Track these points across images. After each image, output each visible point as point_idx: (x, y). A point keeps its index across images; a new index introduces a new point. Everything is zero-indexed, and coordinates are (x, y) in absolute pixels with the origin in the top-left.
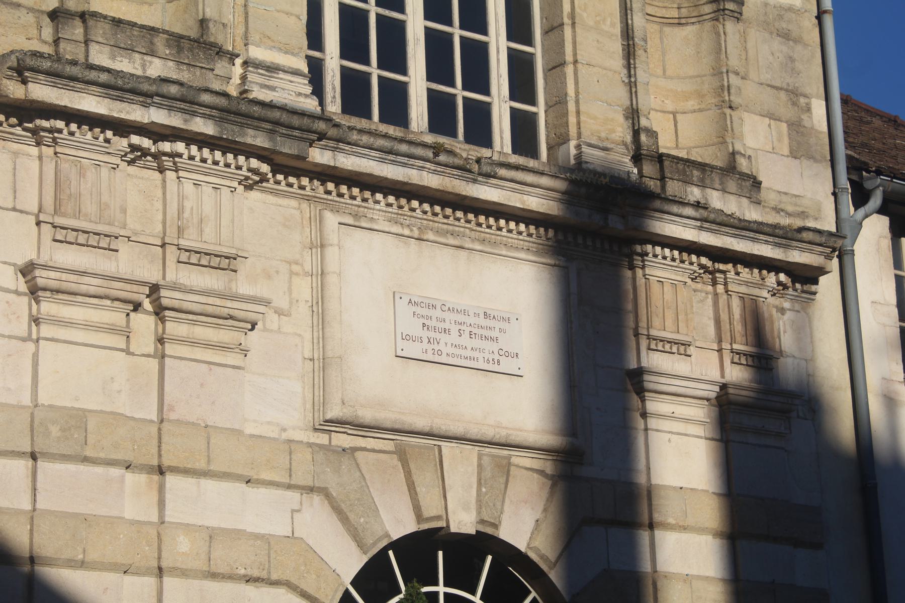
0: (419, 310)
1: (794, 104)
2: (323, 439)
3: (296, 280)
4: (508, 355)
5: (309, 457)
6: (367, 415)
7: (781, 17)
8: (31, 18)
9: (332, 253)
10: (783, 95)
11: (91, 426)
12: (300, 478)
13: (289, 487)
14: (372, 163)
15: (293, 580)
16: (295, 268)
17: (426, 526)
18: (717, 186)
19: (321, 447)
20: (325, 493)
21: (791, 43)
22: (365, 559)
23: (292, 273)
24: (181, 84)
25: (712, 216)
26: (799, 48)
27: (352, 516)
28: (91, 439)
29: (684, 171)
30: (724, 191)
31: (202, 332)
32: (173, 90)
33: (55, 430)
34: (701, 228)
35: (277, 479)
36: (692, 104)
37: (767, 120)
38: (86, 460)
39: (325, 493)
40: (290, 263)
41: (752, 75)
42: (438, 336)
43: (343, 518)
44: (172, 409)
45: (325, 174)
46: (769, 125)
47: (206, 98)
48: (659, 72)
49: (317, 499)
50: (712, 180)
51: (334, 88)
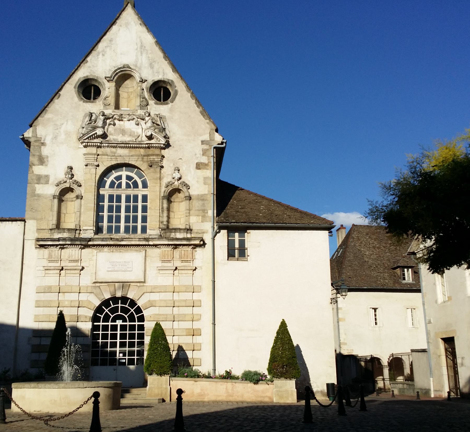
0: (111, 263)
1: (204, 212)
2: (94, 285)
4: (129, 268)
5: (91, 288)
6: (100, 281)
7: (202, 197)
8: (47, 231)
10: (201, 211)
13: (87, 293)
14: (100, 242)
15: (86, 306)
16: (90, 260)
18: (178, 232)
19: (93, 286)
21: (204, 201)
22: (101, 302)
24: (62, 238)
25: (170, 239)
27: (98, 296)
28: (52, 290)
29: (171, 231)
30: (180, 232)
31: (72, 272)
32: (61, 239)
34: (169, 241)
36: (183, 216)
37: (196, 217)
38: (51, 292)
40: (89, 259)
42: (115, 267)
43: (97, 297)
45: (94, 245)
46: (197, 218)
47: (67, 239)
48: (178, 211)
50: (177, 231)
51: (105, 229)
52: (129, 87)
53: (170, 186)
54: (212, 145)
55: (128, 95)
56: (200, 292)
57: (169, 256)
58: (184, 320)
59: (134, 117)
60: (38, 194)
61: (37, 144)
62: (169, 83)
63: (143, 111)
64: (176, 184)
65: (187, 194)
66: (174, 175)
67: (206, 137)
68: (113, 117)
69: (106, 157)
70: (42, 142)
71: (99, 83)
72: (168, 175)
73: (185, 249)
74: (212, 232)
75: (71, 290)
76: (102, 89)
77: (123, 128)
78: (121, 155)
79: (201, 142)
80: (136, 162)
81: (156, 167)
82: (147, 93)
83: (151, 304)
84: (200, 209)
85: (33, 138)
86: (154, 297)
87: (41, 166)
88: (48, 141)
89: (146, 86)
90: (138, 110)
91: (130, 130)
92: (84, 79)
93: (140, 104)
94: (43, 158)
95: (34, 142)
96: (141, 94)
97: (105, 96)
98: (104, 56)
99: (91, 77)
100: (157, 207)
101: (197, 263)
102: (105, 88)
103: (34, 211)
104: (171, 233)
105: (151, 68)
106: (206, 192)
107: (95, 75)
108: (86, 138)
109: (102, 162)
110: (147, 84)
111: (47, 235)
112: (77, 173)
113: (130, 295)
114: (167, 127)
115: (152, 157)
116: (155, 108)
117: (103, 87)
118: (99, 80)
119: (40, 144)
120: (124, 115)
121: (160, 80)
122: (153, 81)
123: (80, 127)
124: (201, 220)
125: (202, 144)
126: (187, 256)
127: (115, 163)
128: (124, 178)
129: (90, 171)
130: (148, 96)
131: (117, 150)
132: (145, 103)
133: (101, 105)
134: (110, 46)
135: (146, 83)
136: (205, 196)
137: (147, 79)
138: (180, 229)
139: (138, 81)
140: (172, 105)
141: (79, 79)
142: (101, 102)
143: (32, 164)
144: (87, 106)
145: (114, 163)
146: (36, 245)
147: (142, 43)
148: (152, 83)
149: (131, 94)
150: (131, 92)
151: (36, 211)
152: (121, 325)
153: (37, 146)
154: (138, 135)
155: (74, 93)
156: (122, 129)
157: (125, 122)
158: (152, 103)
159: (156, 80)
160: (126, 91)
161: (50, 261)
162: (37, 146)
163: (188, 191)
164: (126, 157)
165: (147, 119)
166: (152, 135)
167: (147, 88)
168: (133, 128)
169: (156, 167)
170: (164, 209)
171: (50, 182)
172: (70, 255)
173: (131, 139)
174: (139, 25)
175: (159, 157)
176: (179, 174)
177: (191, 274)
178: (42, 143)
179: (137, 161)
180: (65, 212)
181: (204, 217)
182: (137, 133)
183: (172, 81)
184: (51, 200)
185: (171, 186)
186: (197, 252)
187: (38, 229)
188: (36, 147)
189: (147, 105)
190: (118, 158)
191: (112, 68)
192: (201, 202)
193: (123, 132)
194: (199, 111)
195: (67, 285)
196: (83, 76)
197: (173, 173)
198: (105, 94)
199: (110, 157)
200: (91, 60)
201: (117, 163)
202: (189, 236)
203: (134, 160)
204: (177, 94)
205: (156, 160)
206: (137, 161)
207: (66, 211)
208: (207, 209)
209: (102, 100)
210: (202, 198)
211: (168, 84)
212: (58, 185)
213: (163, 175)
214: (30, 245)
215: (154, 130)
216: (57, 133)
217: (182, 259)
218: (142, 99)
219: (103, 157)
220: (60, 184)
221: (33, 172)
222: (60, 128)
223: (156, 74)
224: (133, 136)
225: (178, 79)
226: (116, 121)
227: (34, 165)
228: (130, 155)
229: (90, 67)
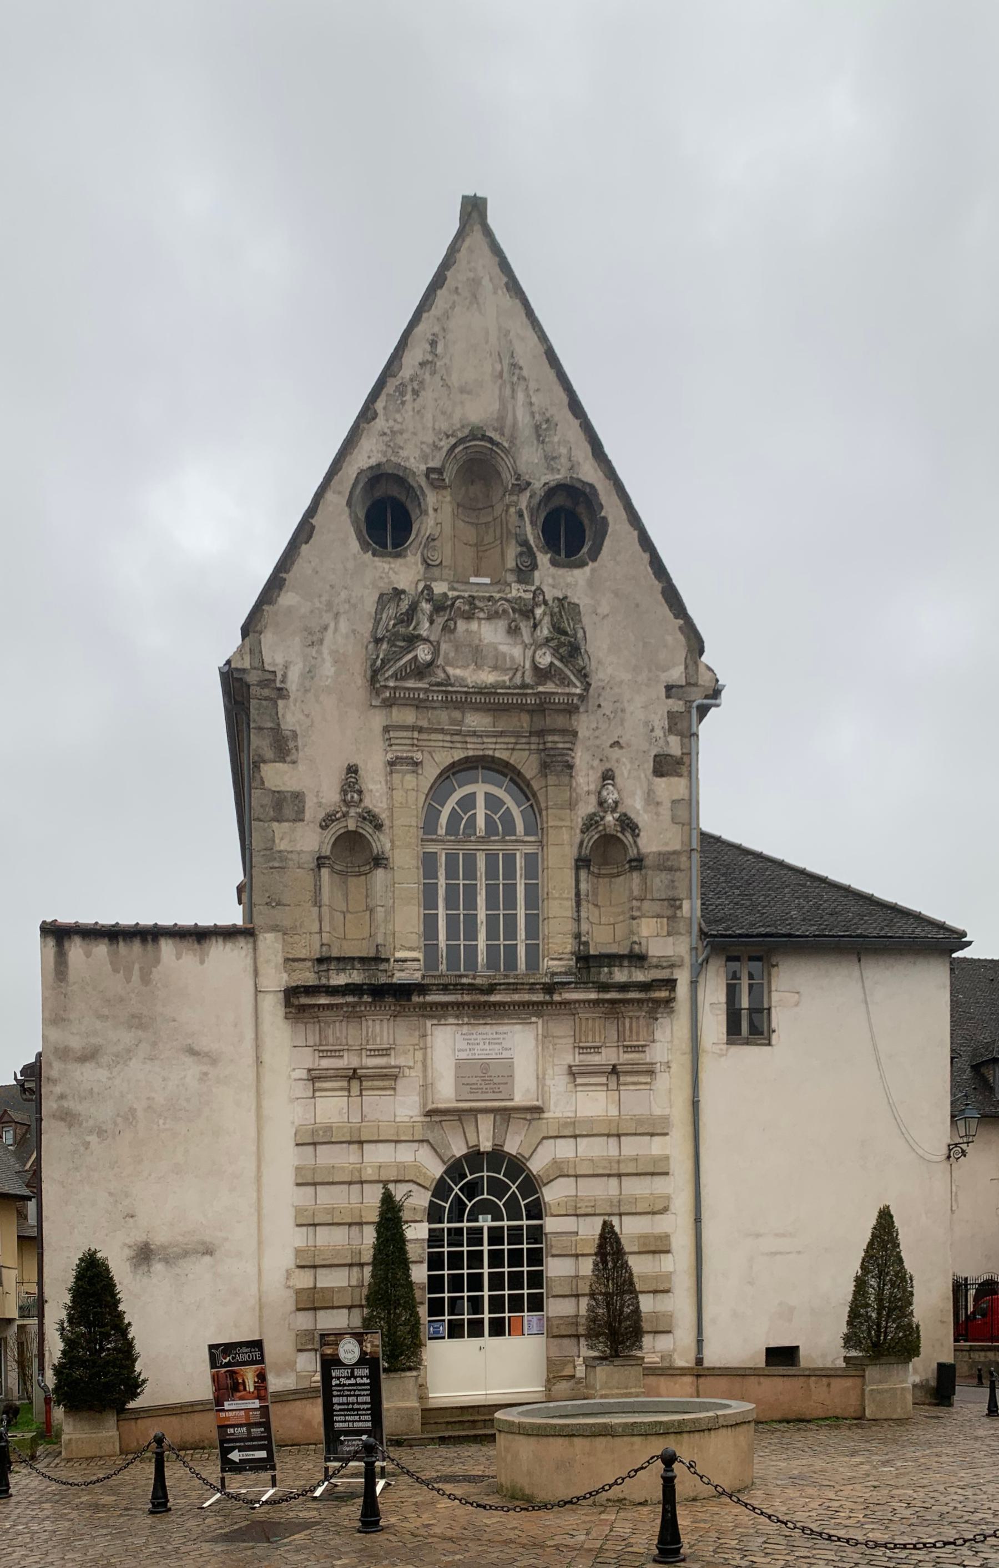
3: (417, 1052)
9: (429, 1038)
10: (666, 903)
11: (334, 1129)
12: (415, 1138)
15: (415, 1179)
17: (471, 1150)
20: (427, 1141)
23: (415, 1050)
26: (678, 873)
27: (438, 1150)
33: (321, 1133)
35: (407, 1139)
37: (655, 919)
39: (427, 1141)
40: (414, 1045)
41: (649, 897)
44: (365, 1116)
49: (425, 1144)
53: (593, 827)
54: (694, 701)
56: (666, 1134)
57: (597, 1034)
58: (634, 1211)
60: (280, 852)
61: (266, 692)
64: (610, 821)
65: (632, 853)
66: (604, 793)
67: (676, 674)
69: (440, 737)
70: (278, 685)
71: (409, 489)
72: (588, 793)
73: (630, 1014)
74: (692, 965)
75: (379, 1136)
76: (418, 511)
77: (477, 642)
78: (475, 732)
79: (664, 690)
80: (511, 754)
81: (559, 769)
82: (533, 530)
83: (561, 1171)
84: (664, 897)
85: (255, 671)
86: (564, 1150)
87: (279, 765)
88: (293, 682)
89: (529, 502)
91: (496, 649)
92: (369, 474)
93: (517, 564)
94: (283, 737)
95: (257, 685)
97: (428, 534)
98: (418, 396)
100: (566, 892)
101: (657, 1053)
103: (274, 904)
104: (600, 967)
105: (538, 440)
106: (678, 847)
109: (430, 753)
111: (307, 977)
112: (371, 787)
113: (511, 1147)
115: (550, 738)
117: (419, 505)
118: (410, 480)
119: (273, 695)
120: (480, 601)
122: (546, 488)
124: (666, 928)
125: (668, 697)
126: (638, 1034)
127: (462, 756)
128: (480, 801)
129: (402, 782)
133: (420, 566)
134: (431, 362)
136: (675, 856)
138: (622, 957)
140: (593, 570)
143: (259, 756)
144: (384, 568)
145: (458, 755)
146: (288, 1004)
147: (515, 355)
151: (279, 904)
152: (490, 1228)
153: (266, 699)
157: (483, 622)
159: (552, 484)
161: (326, 1054)
162: (266, 699)
163: (635, 842)
164: (487, 736)
167: (534, 512)
168: (500, 644)
169: (559, 769)
170: (582, 897)
171: (308, 815)
172: (370, 1035)
173: (500, 679)
174: (505, 290)
175: (567, 739)
176: (616, 792)
177: (646, 1083)
178: (280, 689)
179: (513, 749)
180: (345, 910)
181: (672, 918)
182: (512, 658)
183: (592, 486)
184: (312, 870)
185: (597, 827)
186: (660, 1020)
187: (287, 960)
188: (264, 703)
190: (468, 739)
191: (441, 440)
192: (664, 876)
193: (477, 655)
194: (660, 589)
195: (366, 1119)
197: (599, 787)
198: (427, 529)
199: (448, 738)
200: (385, 408)
201: (466, 755)
202: (640, 976)
205: (561, 746)
206: (513, 749)
207: (347, 904)
208: (681, 896)
209: (421, 547)
210: (666, 863)
212: (327, 826)
213: (577, 794)
214: (272, 1007)
216: (313, 658)
217: (625, 1041)
218: (519, 549)
219: (433, 736)
220: (333, 821)
221: (263, 783)
222: (321, 641)
224: (505, 670)
226: (461, 625)
227: (264, 762)
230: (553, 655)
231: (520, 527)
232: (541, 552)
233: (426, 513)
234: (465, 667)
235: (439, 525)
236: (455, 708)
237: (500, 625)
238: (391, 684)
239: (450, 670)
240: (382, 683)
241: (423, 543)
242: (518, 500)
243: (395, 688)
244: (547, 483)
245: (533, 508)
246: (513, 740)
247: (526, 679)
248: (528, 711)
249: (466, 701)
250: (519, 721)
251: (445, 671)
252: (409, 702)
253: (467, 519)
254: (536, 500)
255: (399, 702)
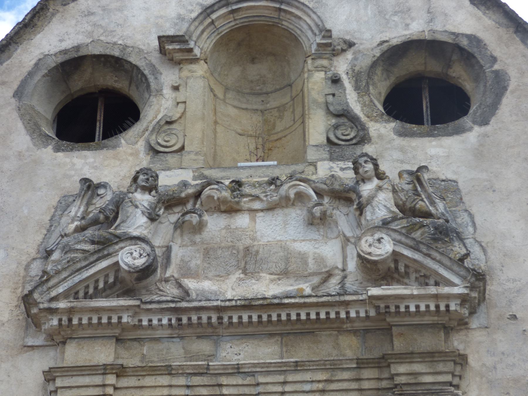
52: (269, 90)
55: (266, 121)
59: (303, 187)
62: (461, 49)
63: (341, 164)
68: (198, 195)
69: (164, 380)
77: (248, 242)
82: (360, 96)
90: (319, 164)
91: (284, 248)
92: (61, 59)
93: (329, 140)
96: (330, 98)
97: (159, 117)
99: (97, 50)
102: (162, 87)
107: (115, 40)
108: (61, 289)
110: (355, 59)
114: (471, 229)
115: (402, 369)
116: (402, 150)
118: (133, 59)
121: (415, 38)
122: (385, 46)
123: (33, 254)
130: (364, 105)
131: (217, 344)
132: (352, 135)
133: (142, 155)
135: (349, 55)
137: (355, 41)
139: (314, 47)
141: (40, 60)
142: (141, 145)
144: (74, 165)
148: (378, 55)
149: (281, 117)
150: (281, 109)
154: (324, 270)
155: (15, 115)
156: (241, 248)
157: (261, 214)
158: (383, 131)
159: (395, 42)
160: (255, 107)
164: (268, 373)
165: (366, 189)
166: (396, 256)
173: (290, 288)
175: (441, 367)
182: (320, 260)
183: (473, 39)
189: (358, 139)
190: (224, 380)
196: (57, 50)
198: (159, 111)
199: (182, 381)
203: (307, 387)
204: (505, 89)
211: (455, 57)
215: (404, 231)
218: (334, 121)
223: (396, 18)
225: (502, 31)
228: (285, 364)
229: (91, 14)
230: (397, 242)
231: (334, 95)
232: (376, 121)
233: (159, 92)
234: (221, 277)
235: (181, 106)
236: (199, 337)
237: (294, 215)
238: (62, 305)
239: (191, 284)
240: (46, 305)
241: (150, 129)
242: (331, 65)
243: (71, 311)
244: (386, 41)
245: (359, 73)
246: (322, 376)
247: (347, 285)
248: (355, 332)
249: (221, 323)
250: (337, 346)
251: (180, 286)
252: (99, 332)
253: (244, 106)
254: (365, 62)
255: (81, 333)
